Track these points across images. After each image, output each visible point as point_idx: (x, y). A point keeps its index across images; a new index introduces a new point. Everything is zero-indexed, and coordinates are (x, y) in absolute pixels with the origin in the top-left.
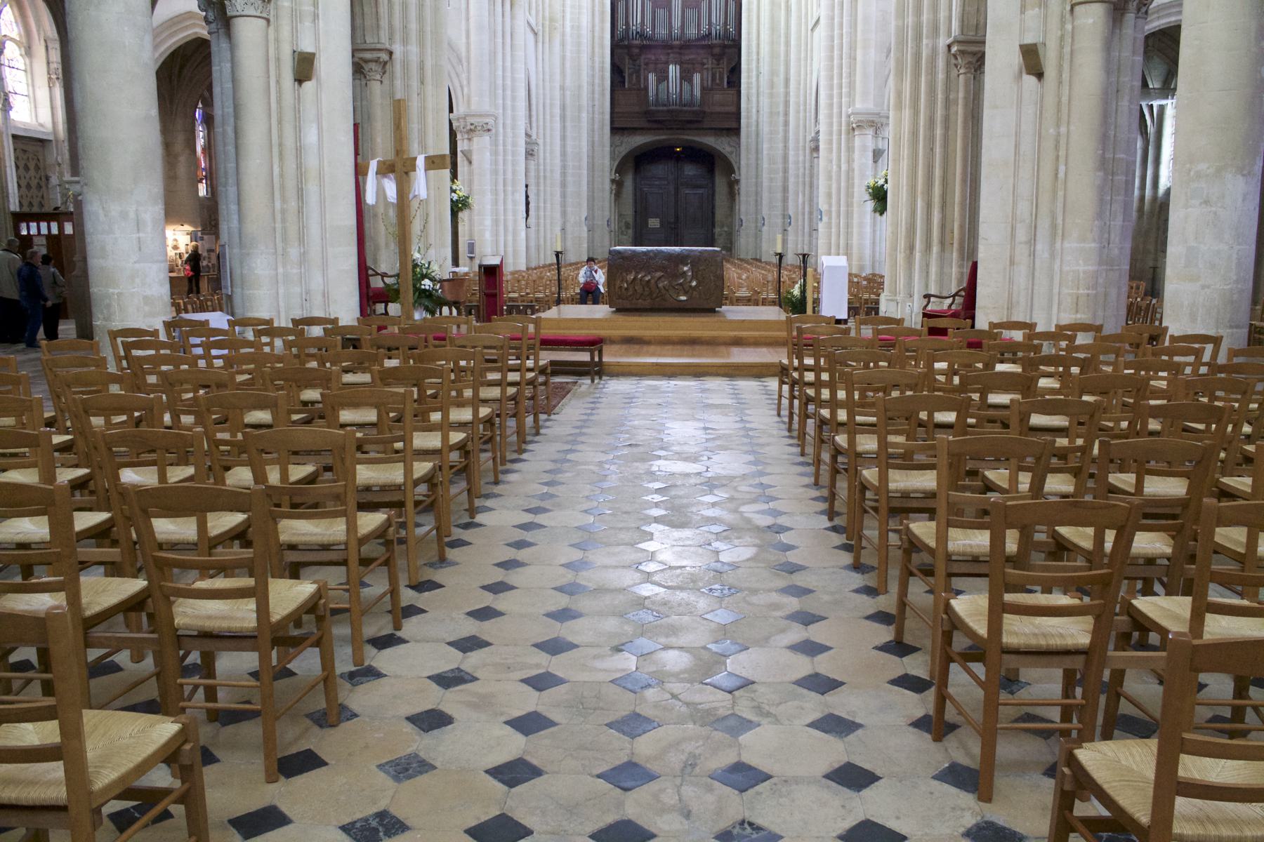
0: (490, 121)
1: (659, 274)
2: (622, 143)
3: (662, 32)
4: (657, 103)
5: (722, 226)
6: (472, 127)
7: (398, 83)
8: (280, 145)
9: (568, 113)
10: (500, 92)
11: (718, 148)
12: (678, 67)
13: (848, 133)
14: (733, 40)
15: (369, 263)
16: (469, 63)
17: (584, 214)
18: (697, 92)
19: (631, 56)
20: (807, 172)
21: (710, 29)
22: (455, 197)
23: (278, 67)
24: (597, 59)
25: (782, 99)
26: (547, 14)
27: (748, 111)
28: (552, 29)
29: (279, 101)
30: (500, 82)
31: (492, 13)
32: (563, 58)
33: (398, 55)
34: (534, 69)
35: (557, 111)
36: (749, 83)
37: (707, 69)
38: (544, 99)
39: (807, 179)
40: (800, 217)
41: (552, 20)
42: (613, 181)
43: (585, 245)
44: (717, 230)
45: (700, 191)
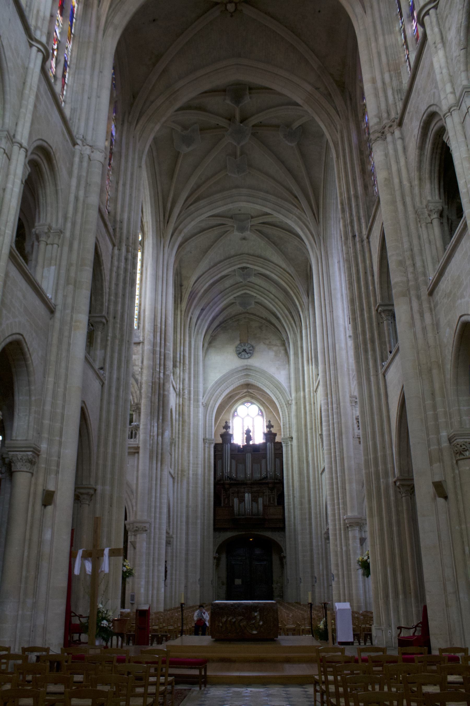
0: (147, 525)
1: (240, 618)
3: (241, 476)
4: (239, 515)
6: (137, 529)
7: (98, 506)
8: (30, 540)
9: (190, 521)
10: (153, 510)
12: (250, 495)
13: (345, 530)
14: (280, 480)
15: (73, 609)
16: (137, 493)
21: (267, 474)
22: (125, 569)
23: (35, 498)
24: (206, 491)
25: (307, 511)
26: (180, 468)
27: (289, 517)
28: (183, 475)
29: (33, 516)
30: (153, 504)
31: (151, 468)
32: (188, 490)
33: (99, 491)
34: (172, 497)
35: (184, 519)
36: (289, 503)
37: (266, 495)
38: (177, 513)
41: (182, 471)
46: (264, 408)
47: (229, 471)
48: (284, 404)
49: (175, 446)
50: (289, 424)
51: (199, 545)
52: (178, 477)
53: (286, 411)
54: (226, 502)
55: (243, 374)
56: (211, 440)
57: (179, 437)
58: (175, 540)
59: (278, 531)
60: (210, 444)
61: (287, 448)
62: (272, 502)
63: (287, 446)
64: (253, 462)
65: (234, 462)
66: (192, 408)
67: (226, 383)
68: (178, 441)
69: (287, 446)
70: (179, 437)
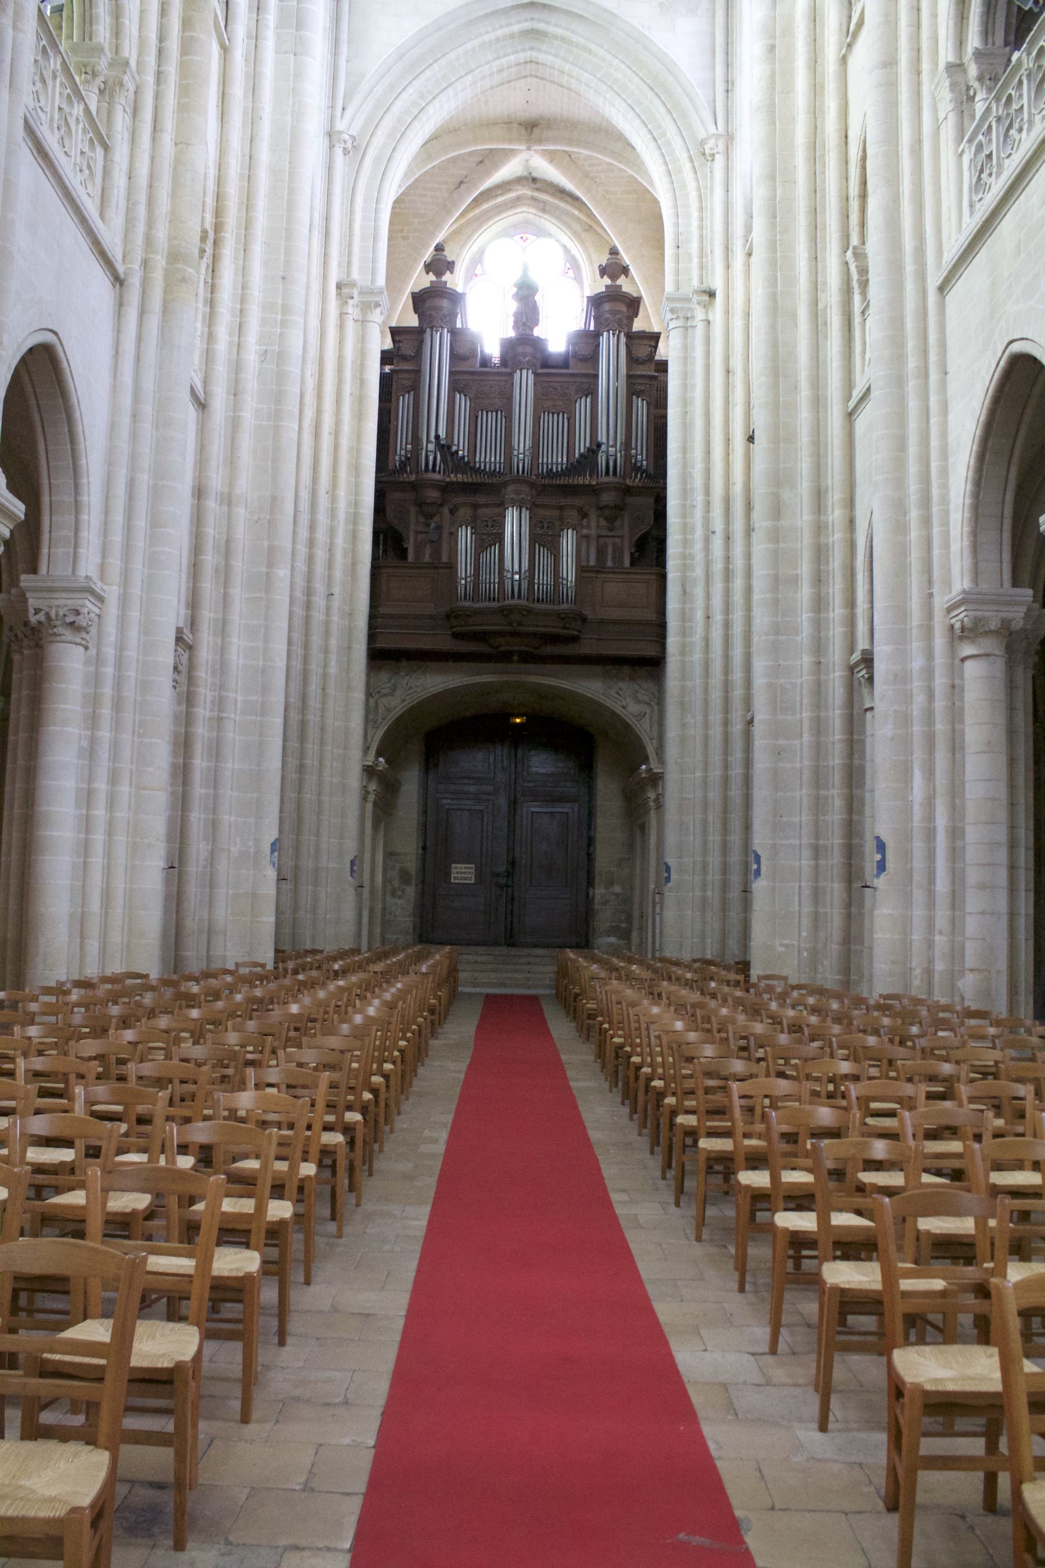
2: (394, 689)
3: (488, 457)
4: (476, 596)
5: (610, 883)
11: (609, 703)
12: (526, 514)
17: (271, 833)
18: (569, 571)
19: (420, 504)
20: (940, 704)
24: (342, 493)
25: (806, 540)
27: (685, 617)
36: (686, 558)
39: (940, 726)
40: (918, 845)
42: (369, 771)
43: (269, 919)
44: (599, 892)
45: (565, 808)
46: (586, 249)
47: (442, 433)
48: (685, 155)
49: (135, 112)
50: (701, 236)
51: (279, 681)
52: (145, 282)
53: (691, 185)
54: (427, 558)
55: (516, 28)
56: (371, 293)
57: (160, 76)
58: (112, 610)
59: (632, 679)
60: (366, 307)
61: (685, 338)
62: (609, 564)
63: (687, 330)
64: (542, 404)
65: (462, 403)
66: (269, 45)
67: (444, 61)
68: (158, 96)
69: (687, 330)
70: (160, 76)
